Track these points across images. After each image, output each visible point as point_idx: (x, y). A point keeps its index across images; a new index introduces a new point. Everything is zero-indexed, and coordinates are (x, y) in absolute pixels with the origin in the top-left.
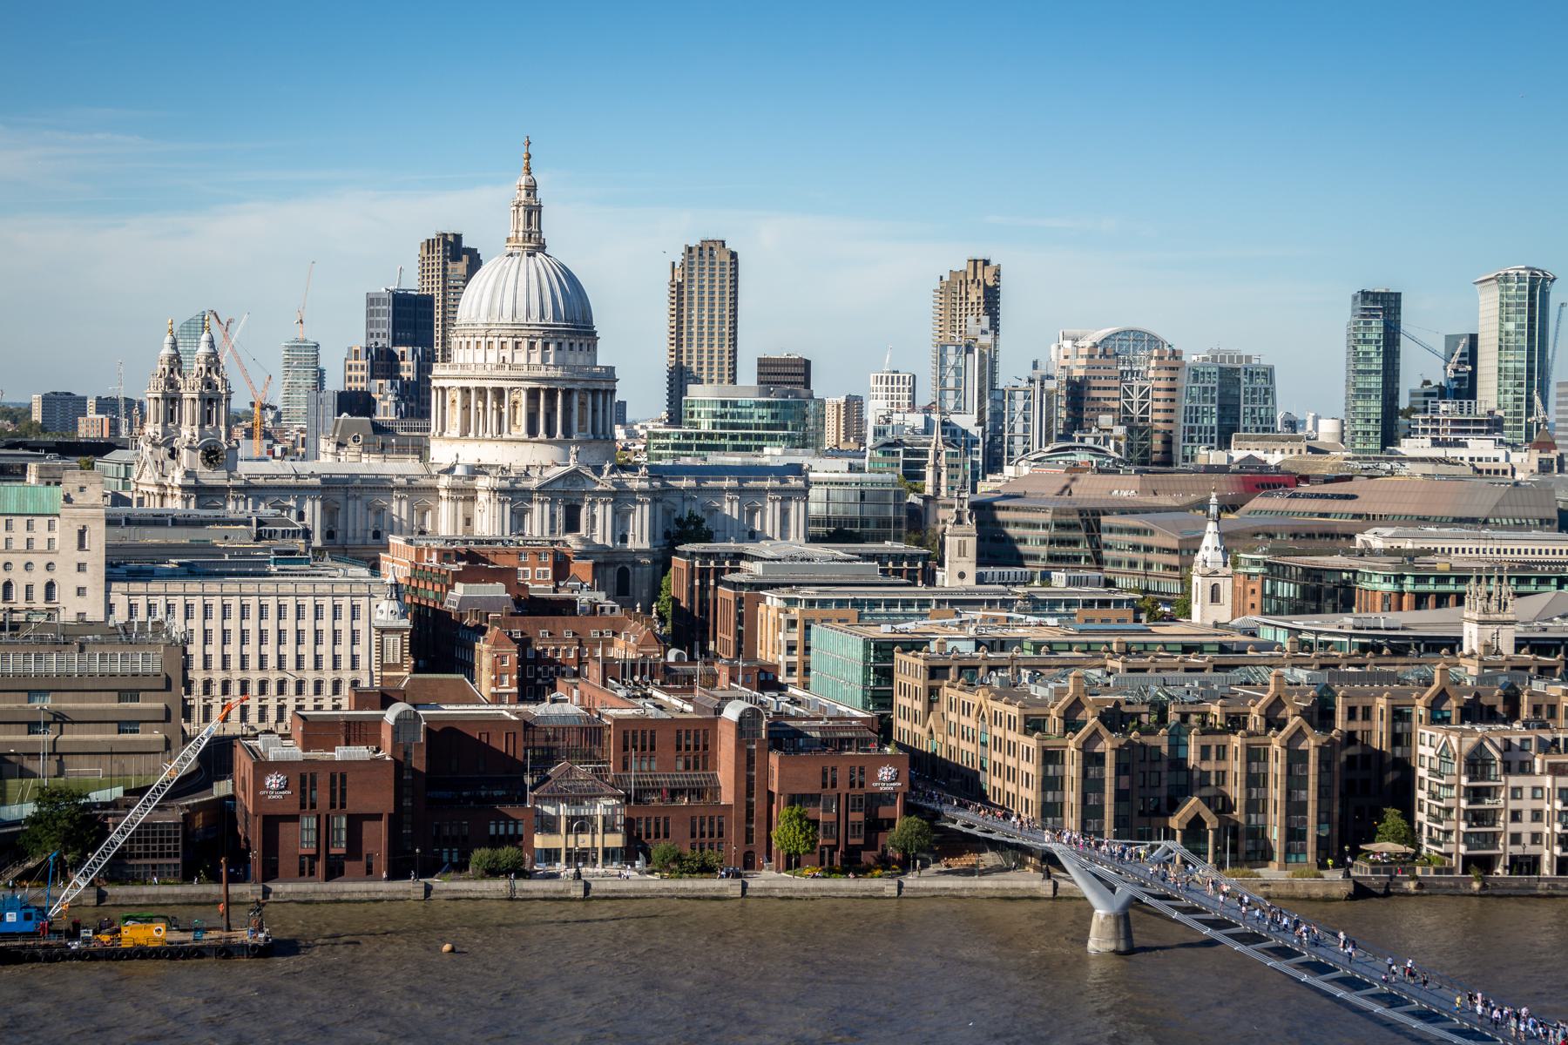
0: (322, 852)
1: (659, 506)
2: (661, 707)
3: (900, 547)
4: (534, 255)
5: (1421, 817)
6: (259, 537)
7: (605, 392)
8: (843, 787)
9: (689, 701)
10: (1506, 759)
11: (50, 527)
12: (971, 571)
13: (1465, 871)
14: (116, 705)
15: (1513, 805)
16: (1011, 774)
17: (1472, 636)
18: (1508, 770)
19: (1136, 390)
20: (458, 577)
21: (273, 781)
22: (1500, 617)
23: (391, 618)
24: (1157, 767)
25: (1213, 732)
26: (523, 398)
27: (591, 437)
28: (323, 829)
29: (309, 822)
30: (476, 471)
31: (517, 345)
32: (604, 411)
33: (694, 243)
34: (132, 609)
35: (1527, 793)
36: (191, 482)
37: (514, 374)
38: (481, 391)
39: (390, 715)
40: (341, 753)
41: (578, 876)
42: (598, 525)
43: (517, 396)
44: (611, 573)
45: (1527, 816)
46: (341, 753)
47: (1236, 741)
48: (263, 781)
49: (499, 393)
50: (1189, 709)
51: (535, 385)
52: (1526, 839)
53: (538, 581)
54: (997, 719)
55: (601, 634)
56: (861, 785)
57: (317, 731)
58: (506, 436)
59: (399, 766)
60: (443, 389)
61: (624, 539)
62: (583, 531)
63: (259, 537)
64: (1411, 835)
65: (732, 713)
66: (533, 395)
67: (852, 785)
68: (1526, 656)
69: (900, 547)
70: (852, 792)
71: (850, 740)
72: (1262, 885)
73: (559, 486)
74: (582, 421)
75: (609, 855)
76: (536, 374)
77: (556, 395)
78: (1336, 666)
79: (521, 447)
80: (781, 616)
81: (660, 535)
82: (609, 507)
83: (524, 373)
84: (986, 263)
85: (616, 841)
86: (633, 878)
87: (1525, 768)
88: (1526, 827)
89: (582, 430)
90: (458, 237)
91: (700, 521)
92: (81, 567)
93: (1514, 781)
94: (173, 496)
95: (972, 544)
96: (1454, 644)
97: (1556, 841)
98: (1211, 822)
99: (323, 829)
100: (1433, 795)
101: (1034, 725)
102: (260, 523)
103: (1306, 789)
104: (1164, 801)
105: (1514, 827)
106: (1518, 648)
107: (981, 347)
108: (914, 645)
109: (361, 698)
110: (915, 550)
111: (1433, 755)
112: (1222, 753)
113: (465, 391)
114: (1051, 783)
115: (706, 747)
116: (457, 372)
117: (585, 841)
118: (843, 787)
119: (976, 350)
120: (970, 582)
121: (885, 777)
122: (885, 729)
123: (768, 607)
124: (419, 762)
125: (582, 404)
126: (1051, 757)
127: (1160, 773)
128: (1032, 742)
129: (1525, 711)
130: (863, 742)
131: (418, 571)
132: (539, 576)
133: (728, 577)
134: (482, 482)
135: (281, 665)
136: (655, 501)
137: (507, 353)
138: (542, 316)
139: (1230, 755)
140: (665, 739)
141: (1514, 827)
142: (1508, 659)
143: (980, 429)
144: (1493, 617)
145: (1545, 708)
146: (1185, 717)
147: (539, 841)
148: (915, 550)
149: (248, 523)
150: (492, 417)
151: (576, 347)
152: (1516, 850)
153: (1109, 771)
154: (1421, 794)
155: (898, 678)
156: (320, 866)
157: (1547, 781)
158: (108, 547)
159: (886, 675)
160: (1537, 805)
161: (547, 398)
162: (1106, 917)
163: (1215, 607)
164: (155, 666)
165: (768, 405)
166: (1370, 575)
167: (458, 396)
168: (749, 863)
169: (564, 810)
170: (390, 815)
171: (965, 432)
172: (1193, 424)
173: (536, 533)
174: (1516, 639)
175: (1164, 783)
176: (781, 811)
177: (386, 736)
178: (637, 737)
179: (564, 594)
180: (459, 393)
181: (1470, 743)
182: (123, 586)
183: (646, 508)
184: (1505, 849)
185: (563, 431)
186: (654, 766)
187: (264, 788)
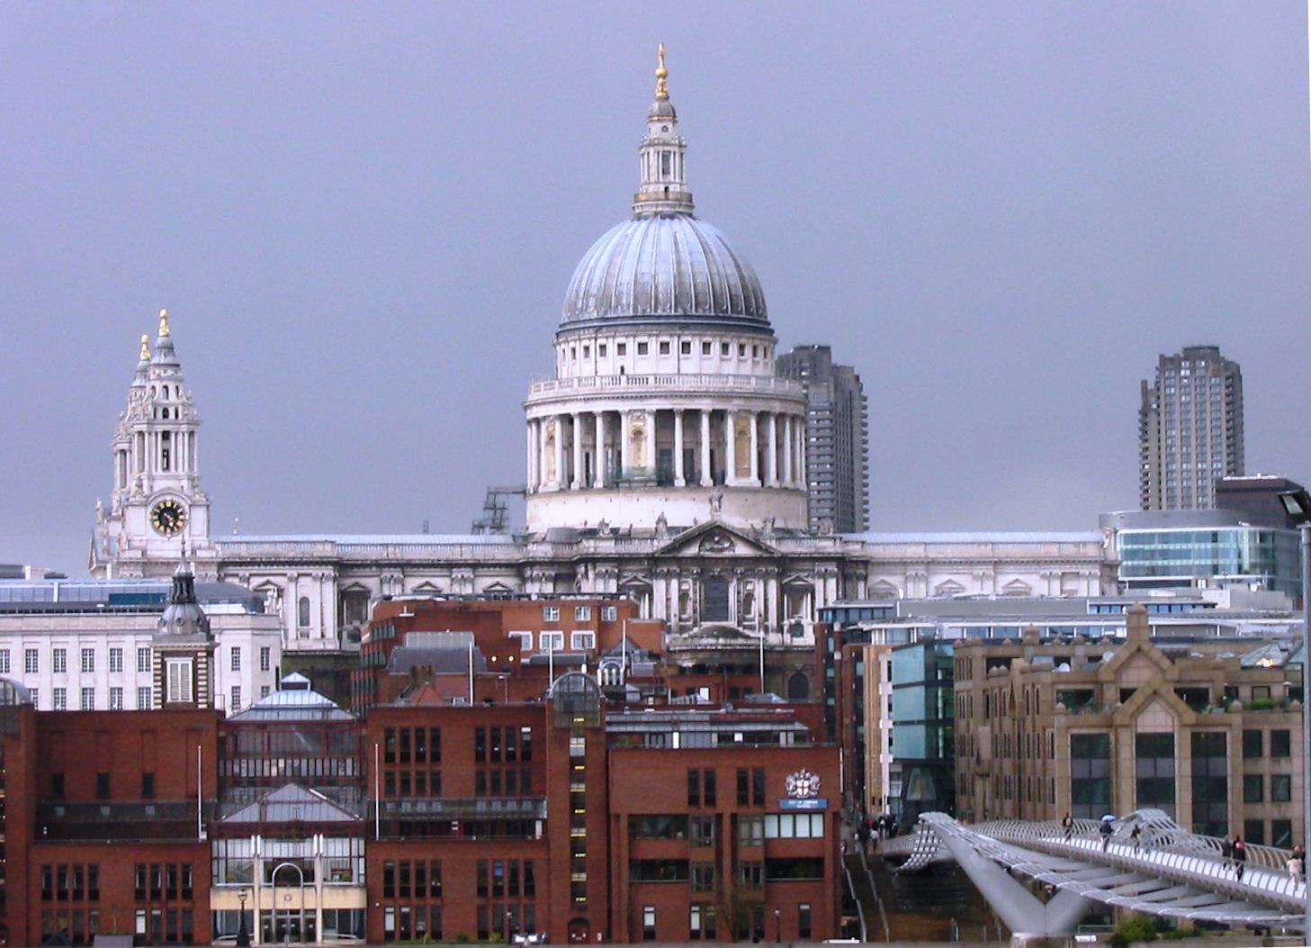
4: (672, 217)
7: (780, 417)
26: (649, 426)
27: (759, 484)
30: (573, 536)
31: (642, 348)
32: (779, 447)
37: (636, 388)
38: (588, 418)
43: (639, 424)
49: (614, 418)
56: (760, 800)
60: (537, 421)
66: (664, 418)
73: (693, 550)
74: (740, 457)
77: (699, 421)
82: (773, 585)
85: (352, 899)
89: (741, 471)
90: (825, 350)
113: (567, 420)
125: (741, 434)
127: (1289, 777)
137: (622, 360)
147: (224, 901)
151: (733, 349)
180: (558, 425)
183: (832, 583)
185: (712, 475)
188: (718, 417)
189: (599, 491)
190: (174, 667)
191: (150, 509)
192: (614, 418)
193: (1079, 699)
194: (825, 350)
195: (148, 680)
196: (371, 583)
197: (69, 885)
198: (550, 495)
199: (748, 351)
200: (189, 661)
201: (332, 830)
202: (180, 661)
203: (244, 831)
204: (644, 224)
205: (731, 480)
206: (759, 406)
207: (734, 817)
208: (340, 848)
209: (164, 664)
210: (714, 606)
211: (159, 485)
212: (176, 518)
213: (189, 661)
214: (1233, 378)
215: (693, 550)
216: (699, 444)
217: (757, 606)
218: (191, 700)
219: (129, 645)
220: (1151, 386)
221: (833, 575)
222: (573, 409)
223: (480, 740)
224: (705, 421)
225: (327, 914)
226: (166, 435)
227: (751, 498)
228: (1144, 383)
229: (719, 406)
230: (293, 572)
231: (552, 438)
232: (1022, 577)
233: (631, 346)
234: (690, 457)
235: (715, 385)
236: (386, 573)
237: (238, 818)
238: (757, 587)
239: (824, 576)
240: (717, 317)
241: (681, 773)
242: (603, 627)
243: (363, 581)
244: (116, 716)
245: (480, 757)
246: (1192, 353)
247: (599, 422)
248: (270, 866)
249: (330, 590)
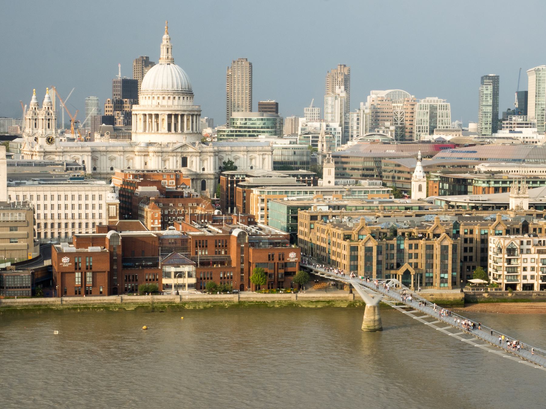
0: (83, 286)
1: (217, 157)
2: (210, 231)
3: (304, 172)
4: (169, 64)
5: (490, 270)
6: (67, 169)
7: (197, 115)
8: (276, 260)
9: (221, 229)
10: (521, 248)
12: (333, 180)
13: (506, 289)
14: (9, 232)
15: (524, 265)
16: (339, 255)
17: (513, 204)
18: (522, 251)
19: (399, 113)
20: (142, 184)
21: (65, 260)
22: (523, 196)
23: (112, 199)
24: (392, 252)
25: (414, 239)
26: (166, 118)
28: (83, 277)
29: (78, 275)
31: (164, 98)
32: (196, 122)
34: (17, 197)
35: (529, 260)
36: (42, 150)
37: (162, 108)
38: (151, 115)
39: (109, 235)
40: (90, 249)
41: (178, 294)
42: (194, 165)
43: (163, 117)
44: (199, 183)
45: (529, 269)
46: (90, 249)
47: (422, 242)
48: (61, 259)
49: (157, 116)
50: (404, 230)
51: (170, 113)
52: (529, 277)
53: (170, 184)
54: (334, 235)
55: (192, 205)
56: (283, 259)
57: (82, 241)
58: (159, 132)
59: (111, 254)
60: (136, 114)
61: (204, 169)
62: (188, 167)
63: (67, 169)
64: (486, 276)
65: (235, 233)
66: (170, 116)
67: (280, 259)
68: (532, 210)
69: (304, 172)
70: (280, 262)
71: (279, 243)
72: (431, 295)
73: (179, 150)
74: (187, 126)
75: (190, 286)
76: (171, 108)
78: (461, 214)
80: (259, 197)
81: (217, 168)
82: (198, 158)
83: (166, 108)
85: (193, 281)
86: (198, 295)
87: (528, 251)
88: (529, 273)
89: (188, 129)
91: (232, 163)
93: (524, 256)
94: (36, 155)
95: (333, 171)
96: (506, 206)
97: (539, 278)
98: (413, 272)
99: (83, 277)
100: (495, 262)
101: (347, 237)
102: (67, 165)
103: (448, 259)
104: (395, 264)
105: (524, 273)
106: (530, 207)
107: (341, 97)
108: (305, 208)
109: (101, 228)
110: (310, 173)
111: (494, 247)
112: (417, 246)
113: (145, 115)
114: (354, 258)
115: (226, 246)
116: (142, 108)
117: (180, 281)
118: (276, 260)
119: (339, 99)
120: (332, 184)
121: (292, 256)
122: (293, 238)
123: (254, 194)
124: (119, 251)
125: (188, 120)
126: (354, 249)
127: (393, 254)
128: (346, 243)
129: (531, 231)
130: (283, 244)
131: (125, 183)
132: (170, 183)
133: (241, 183)
134: (151, 149)
135: (45, 217)
136: (215, 155)
137: (160, 101)
138: (173, 87)
139: (419, 247)
140: (211, 243)
141: (524, 273)
142: (525, 211)
143: (340, 128)
144: (520, 196)
145: (537, 229)
146: (403, 234)
147: (165, 281)
148: (310, 173)
149: (63, 165)
150: (154, 124)
151: (185, 98)
152: (525, 282)
153: (375, 253)
154: (490, 261)
155: (299, 220)
156: (83, 291)
157: (536, 256)
158: (8, 174)
159: (295, 218)
160: (533, 265)
161: (175, 118)
162: (371, 307)
163: (420, 193)
164: (23, 218)
165: (262, 119)
166: (478, 181)
167: (142, 117)
168: (242, 289)
169: (173, 269)
170: (108, 272)
171: (335, 129)
172: (420, 125)
173: (171, 168)
174: (529, 204)
175: (395, 258)
176: (253, 269)
177: (107, 243)
178: (201, 242)
179: (179, 190)
181: (507, 242)
182: (14, 188)
183: (212, 158)
184: (521, 282)
186: (207, 253)
187: (62, 262)
188: (182, 116)
189: (154, 133)
190: (111, 208)
191: (45, 138)
192: (157, 116)
194: (322, 178)
196: (98, 155)
197: (131, 278)
198: (140, 133)
199: (189, 98)
200: (115, 206)
202: (112, 206)
204: (163, 66)
206: (193, 113)
207: (278, 263)
209: (109, 207)
210: (184, 163)
211: (49, 132)
212: (52, 140)
213: (115, 206)
215: (179, 150)
216: (178, 122)
217: (194, 163)
221: (212, 156)
222: (147, 113)
223: (216, 242)
224: (179, 117)
226: (49, 120)
227: (190, 135)
229: (183, 113)
230: (81, 154)
231: (140, 119)
232: (253, 155)
233: (161, 97)
235: (182, 108)
236: (102, 153)
238: (194, 159)
240: (182, 91)
241: (267, 254)
242: (177, 180)
243: (96, 155)
245: (216, 246)
246: (241, 60)
247: (153, 117)
248: (176, 273)
249: (90, 158)
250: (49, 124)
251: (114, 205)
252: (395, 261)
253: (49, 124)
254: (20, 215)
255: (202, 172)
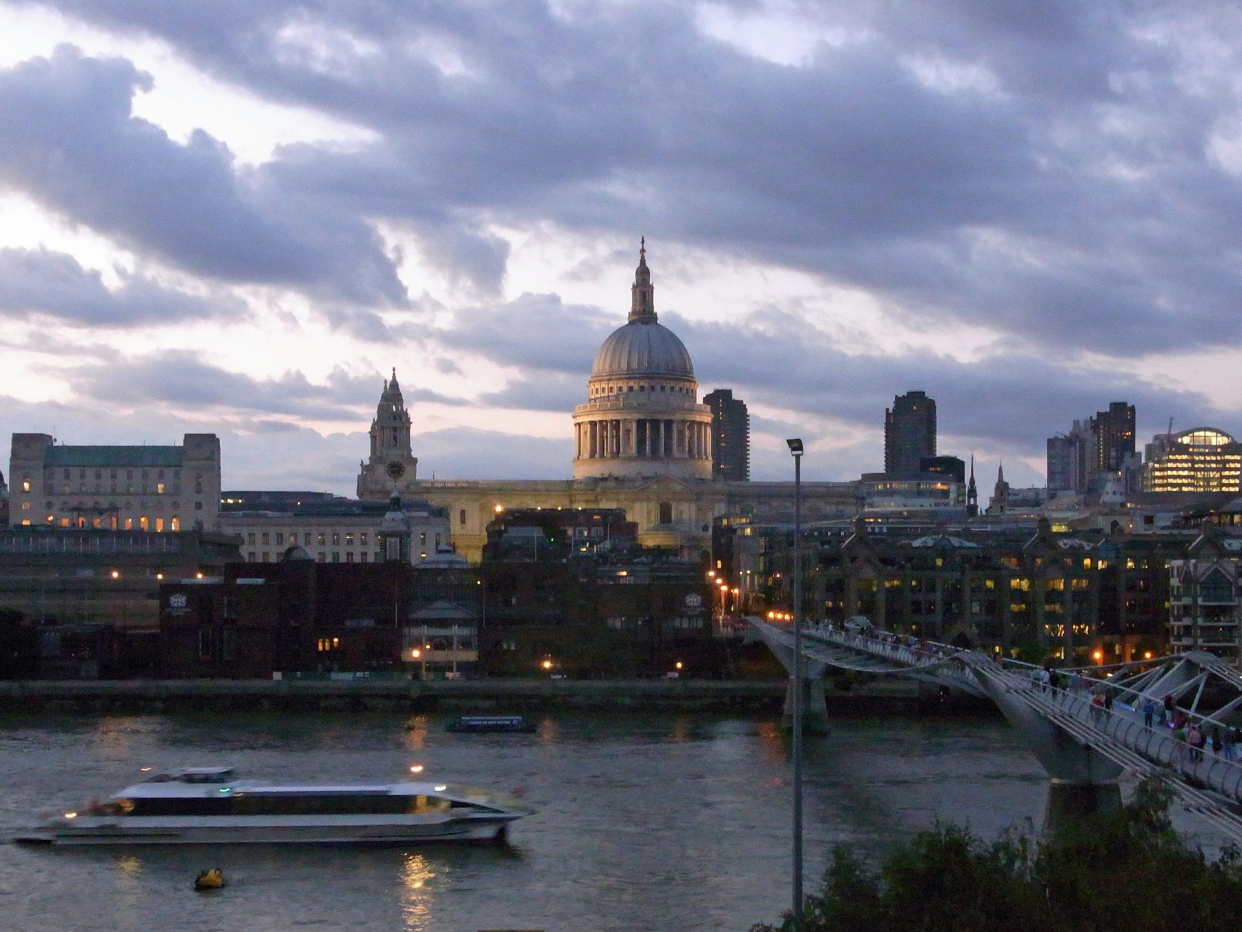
11: (177, 475)
26: (634, 427)
33: (902, 393)
36: (379, 487)
48: (168, 600)
66: (641, 424)
75: (463, 667)
79: (634, 464)
82: (693, 507)
84: (1124, 404)
85: (471, 656)
92: (199, 506)
113: (593, 424)
119: (1078, 444)
161: (651, 429)
180: (589, 426)
187: (169, 606)
193: (829, 561)
195: (378, 550)
200: (397, 540)
201: (463, 623)
202: (393, 540)
203: (419, 623)
205: (675, 453)
208: (465, 632)
213: (398, 540)
214: (930, 406)
218: (399, 558)
219: (371, 531)
220: (891, 411)
224: (662, 426)
225: (458, 663)
228: (887, 410)
231: (586, 433)
234: (655, 442)
237: (415, 616)
239: (719, 501)
244: (363, 565)
250: (395, 438)
251: (397, 536)
252: (938, 618)
253: (395, 438)
254: (168, 543)
255: (701, 534)
